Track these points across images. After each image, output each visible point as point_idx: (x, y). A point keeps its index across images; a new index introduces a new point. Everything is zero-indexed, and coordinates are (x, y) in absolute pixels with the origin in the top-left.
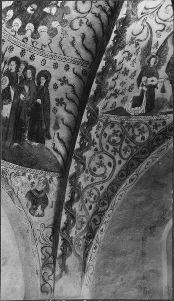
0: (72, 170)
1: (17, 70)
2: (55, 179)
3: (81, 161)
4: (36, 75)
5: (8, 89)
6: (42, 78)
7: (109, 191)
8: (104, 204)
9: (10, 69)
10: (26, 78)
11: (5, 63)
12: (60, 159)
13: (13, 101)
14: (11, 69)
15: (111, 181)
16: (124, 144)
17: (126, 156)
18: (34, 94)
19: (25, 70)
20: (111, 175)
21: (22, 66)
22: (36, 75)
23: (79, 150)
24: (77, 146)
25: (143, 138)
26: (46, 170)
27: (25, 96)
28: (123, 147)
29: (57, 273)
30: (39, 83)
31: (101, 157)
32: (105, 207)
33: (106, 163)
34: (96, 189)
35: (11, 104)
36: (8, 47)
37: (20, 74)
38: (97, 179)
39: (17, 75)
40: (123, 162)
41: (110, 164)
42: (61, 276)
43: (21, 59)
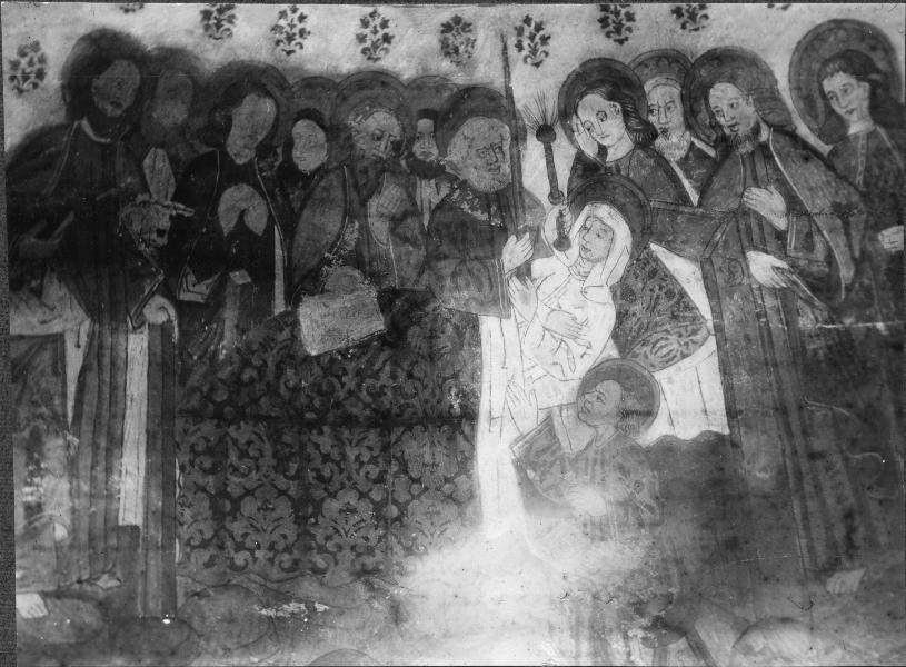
1: (646, 136)
4: (783, 84)
5: (644, 268)
6: (836, 82)
9: (590, 152)
10: (726, 144)
11: (545, 132)
13: (717, 312)
14: (603, 150)
18: (841, 211)
19: (694, 101)
21: (661, 94)
22: (783, 84)
27: (782, 252)
30: (833, 126)
35: (712, 344)
36: (512, 41)
37: (675, 143)
39: (661, 160)
43: (624, 55)
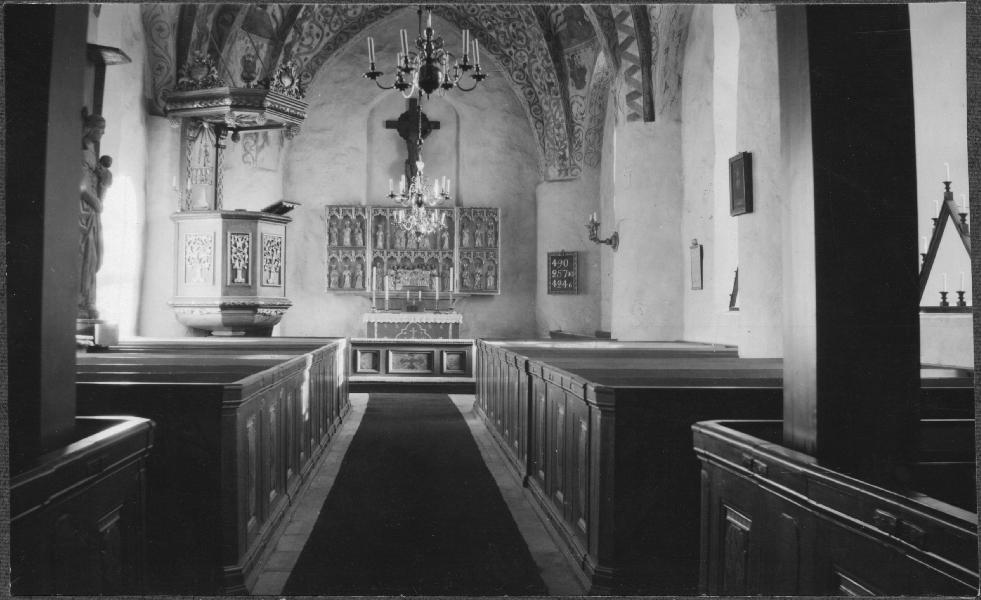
0: (289, 39)
2: (265, 45)
3: (299, 30)
7: (313, 64)
8: (307, 76)
12: (274, 26)
15: (315, 53)
16: (336, 17)
17: (335, 29)
20: (318, 45)
23: (300, 19)
24: (300, 15)
25: (355, 13)
26: (260, 35)
28: (334, 19)
29: (260, 143)
31: (311, 27)
32: (308, 80)
33: (314, 33)
34: (300, 60)
38: (304, 50)
40: (331, 35)
41: (318, 35)
42: (262, 146)
